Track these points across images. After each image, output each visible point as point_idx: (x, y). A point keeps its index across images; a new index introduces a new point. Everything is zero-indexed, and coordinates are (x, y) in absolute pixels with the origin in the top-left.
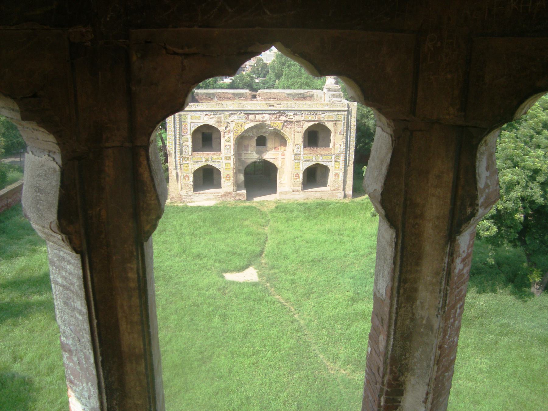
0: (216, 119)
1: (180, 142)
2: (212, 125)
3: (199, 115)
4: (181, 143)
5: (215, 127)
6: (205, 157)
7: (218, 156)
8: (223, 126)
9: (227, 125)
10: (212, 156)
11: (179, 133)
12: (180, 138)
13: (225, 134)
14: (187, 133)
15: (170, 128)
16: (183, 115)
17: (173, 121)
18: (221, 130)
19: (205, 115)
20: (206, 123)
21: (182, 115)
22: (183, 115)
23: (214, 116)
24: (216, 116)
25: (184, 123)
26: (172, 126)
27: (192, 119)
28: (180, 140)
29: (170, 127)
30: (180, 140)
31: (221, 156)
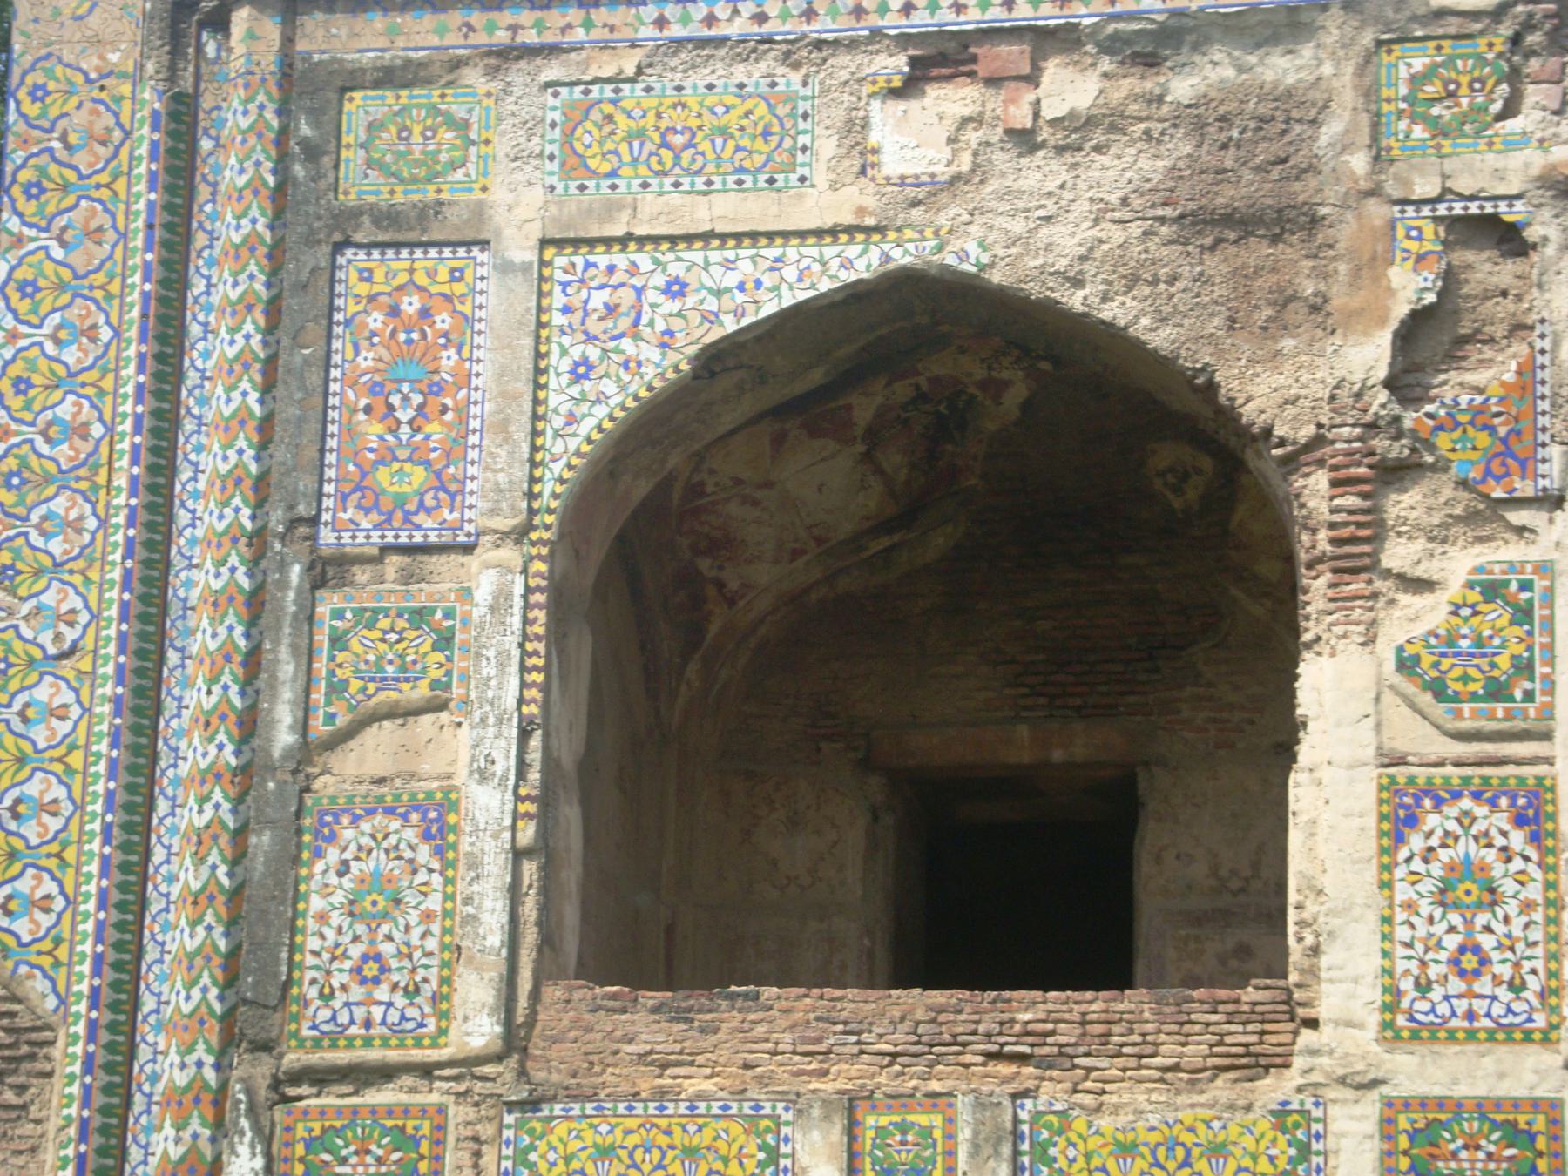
0: (1181, 146)
1: (250, 725)
2: (1075, 300)
3: (752, 74)
4: (284, 738)
5: (1161, 339)
6: (851, 1106)
7: (1197, 1077)
8: (1362, 319)
9: (1450, 280)
10: (1052, 1093)
11: (262, 491)
12: (256, 606)
13: (1404, 504)
14: (447, 488)
15: (65, 411)
16: (391, 77)
17: (140, 254)
18: (1294, 428)
19: (895, 64)
20: (902, 257)
21: (351, 80)
22: (391, 77)
23: (1131, 84)
24: (1182, 87)
25: (391, 268)
26: (107, 364)
27: (574, 164)
28: (253, 664)
29: (68, 380)
30: (253, 664)
31: (1274, 1089)
